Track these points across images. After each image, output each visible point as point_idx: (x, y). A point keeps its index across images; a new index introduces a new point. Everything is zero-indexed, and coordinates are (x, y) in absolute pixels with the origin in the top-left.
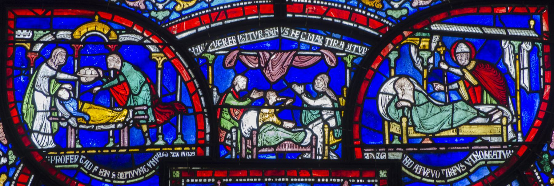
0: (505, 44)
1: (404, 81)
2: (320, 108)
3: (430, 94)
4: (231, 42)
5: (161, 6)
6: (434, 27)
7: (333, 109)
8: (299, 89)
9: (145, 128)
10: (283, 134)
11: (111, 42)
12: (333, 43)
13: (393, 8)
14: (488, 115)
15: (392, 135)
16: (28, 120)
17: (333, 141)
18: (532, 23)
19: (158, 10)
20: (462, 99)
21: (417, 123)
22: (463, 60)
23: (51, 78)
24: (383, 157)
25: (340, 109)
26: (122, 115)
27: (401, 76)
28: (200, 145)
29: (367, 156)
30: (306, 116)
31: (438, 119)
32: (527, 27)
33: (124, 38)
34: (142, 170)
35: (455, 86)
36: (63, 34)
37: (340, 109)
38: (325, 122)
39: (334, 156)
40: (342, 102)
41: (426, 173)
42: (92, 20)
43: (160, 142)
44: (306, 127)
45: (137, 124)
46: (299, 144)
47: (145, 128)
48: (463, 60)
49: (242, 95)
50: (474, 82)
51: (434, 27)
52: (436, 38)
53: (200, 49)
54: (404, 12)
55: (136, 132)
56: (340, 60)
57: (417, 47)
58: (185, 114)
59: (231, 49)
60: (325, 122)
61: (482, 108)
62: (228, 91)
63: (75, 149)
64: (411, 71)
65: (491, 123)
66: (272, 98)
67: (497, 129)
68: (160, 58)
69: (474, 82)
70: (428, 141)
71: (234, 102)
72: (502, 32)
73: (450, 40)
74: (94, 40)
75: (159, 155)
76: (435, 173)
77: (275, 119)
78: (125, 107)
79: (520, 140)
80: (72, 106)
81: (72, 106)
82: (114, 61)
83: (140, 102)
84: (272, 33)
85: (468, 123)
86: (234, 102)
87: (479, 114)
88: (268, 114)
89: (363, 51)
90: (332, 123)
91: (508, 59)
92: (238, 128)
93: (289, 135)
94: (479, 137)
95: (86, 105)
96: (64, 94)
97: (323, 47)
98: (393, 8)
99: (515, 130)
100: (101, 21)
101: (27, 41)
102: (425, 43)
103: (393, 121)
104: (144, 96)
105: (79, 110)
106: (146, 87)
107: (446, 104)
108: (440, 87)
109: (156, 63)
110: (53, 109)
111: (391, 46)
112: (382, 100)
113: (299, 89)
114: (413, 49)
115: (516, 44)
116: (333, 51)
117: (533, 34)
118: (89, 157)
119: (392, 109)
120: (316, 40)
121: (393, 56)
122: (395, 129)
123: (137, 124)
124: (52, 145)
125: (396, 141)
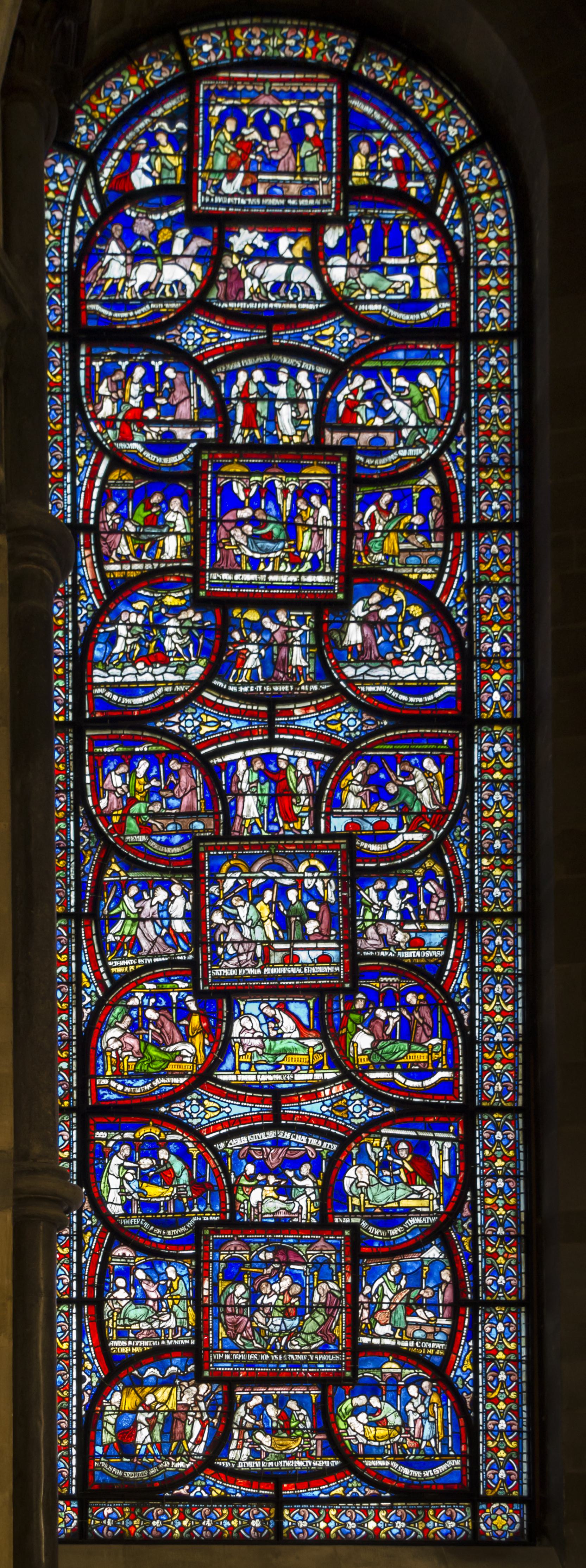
0: (432, 1143)
1: (362, 1169)
2: (305, 1187)
3: (379, 1179)
4: (243, 1140)
5: (195, 1115)
6: (384, 1131)
7: (314, 1188)
8: (290, 1174)
9: (185, 1200)
10: (279, 1205)
11: (161, 1140)
12: (314, 1142)
13: (355, 1117)
14: (419, 1193)
15: (354, 1206)
16: (105, 1195)
17: (313, 1210)
18: (452, 1128)
19: (193, 1118)
20: (402, 1181)
21: (371, 1197)
22: (403, 1154)
23: (120, 1166)
24: (347, 1221)
25: (318, 1187)
26: (169, 1191)
27: (360, 1165)
28: (223, 1212)
29: (336, 1220)
30: (295, 1192)
31: (385, 1195)
32: (448, 1131)
33: (170, 1137)
34: (183, 1229)
35: (397, 1172)
36: (128, 1135)
37: (318, 1187)
38: (308, 1196)
39: (314, 1220)
40: (320, 1182)
41: (377, 1232)
42: (147, 1125)
43: (196, 1210)
44: (295, 1200)
45: (180, 1197)
46: (290, 1212)
47: (185, 1200)
48: (403, 1154)
49: (250, 1178)
50: (410, 1169)
51: (384, 1131)
52: (385, 1139)
53: (222, 1145)
54: (363, 1120)
55: (178, 1203)
56: (319, 1154)
57: (372, 1145)
58: (212, 1190)
59: (243, 1146)
60: (308, 1196)
61: (416, 1188)
62: (241, 1175)
63: (137, 1215)
64: (366, 1161)
65: (422, 1198)
66: (272, 1179)
67: (426, 1203)
68: (195, 1153)
69: (410, 1169)
70: (378, 1210)
71: (246, 1183)
72: (431, 1135)
73: (394, 1140)
74: (149, 1139)
75: (195, 1219)
76: (383, 1233)
77: (274, 1194)
78: (171, 1185)
79: (442, 1210)
80: (135, 1185)
81: (135, 1185)
82: (163, 1154)
83: (181, 1182)
84: (271, 1134)
85: (406, 1198)
86: (246, 1183)
87: (414, 1192)
88: (269, 1191)
89: (335, 1147)
90: (313, 1197)
91: (435, 1153)
92: (249, 1201)
93: (284, 1206)
94: (414, 1208)
95: (145, 1184)
96: (129, 1177)
97: (307, 1145)
98: (355, 1117)
99: (439, 1204)
100: (154, 1125)
101: (102, 1139)
102: (377, 1142)
103: (354, 1196)
104: (184, 1178)
105: (139, 1188)
106: (186, 1172)
107: (391, 1185)
108: (387, 1173)
109: (192, 1155)
110: (122, 1187)
111: (353, 1144)
112: (347, 1182)
113: (290, 1174)
114: (368, 1146)
115: (440, 1143)
116: (314, 1147)
117: (452, 1136)
118: (147, 1220)
119: (354, 1188)
120: (301, 1139)
121: (354, 1151)
122: (356, 1201)
123: (180, 1197)
124: (122, 1212)
125: (356, 1210)
